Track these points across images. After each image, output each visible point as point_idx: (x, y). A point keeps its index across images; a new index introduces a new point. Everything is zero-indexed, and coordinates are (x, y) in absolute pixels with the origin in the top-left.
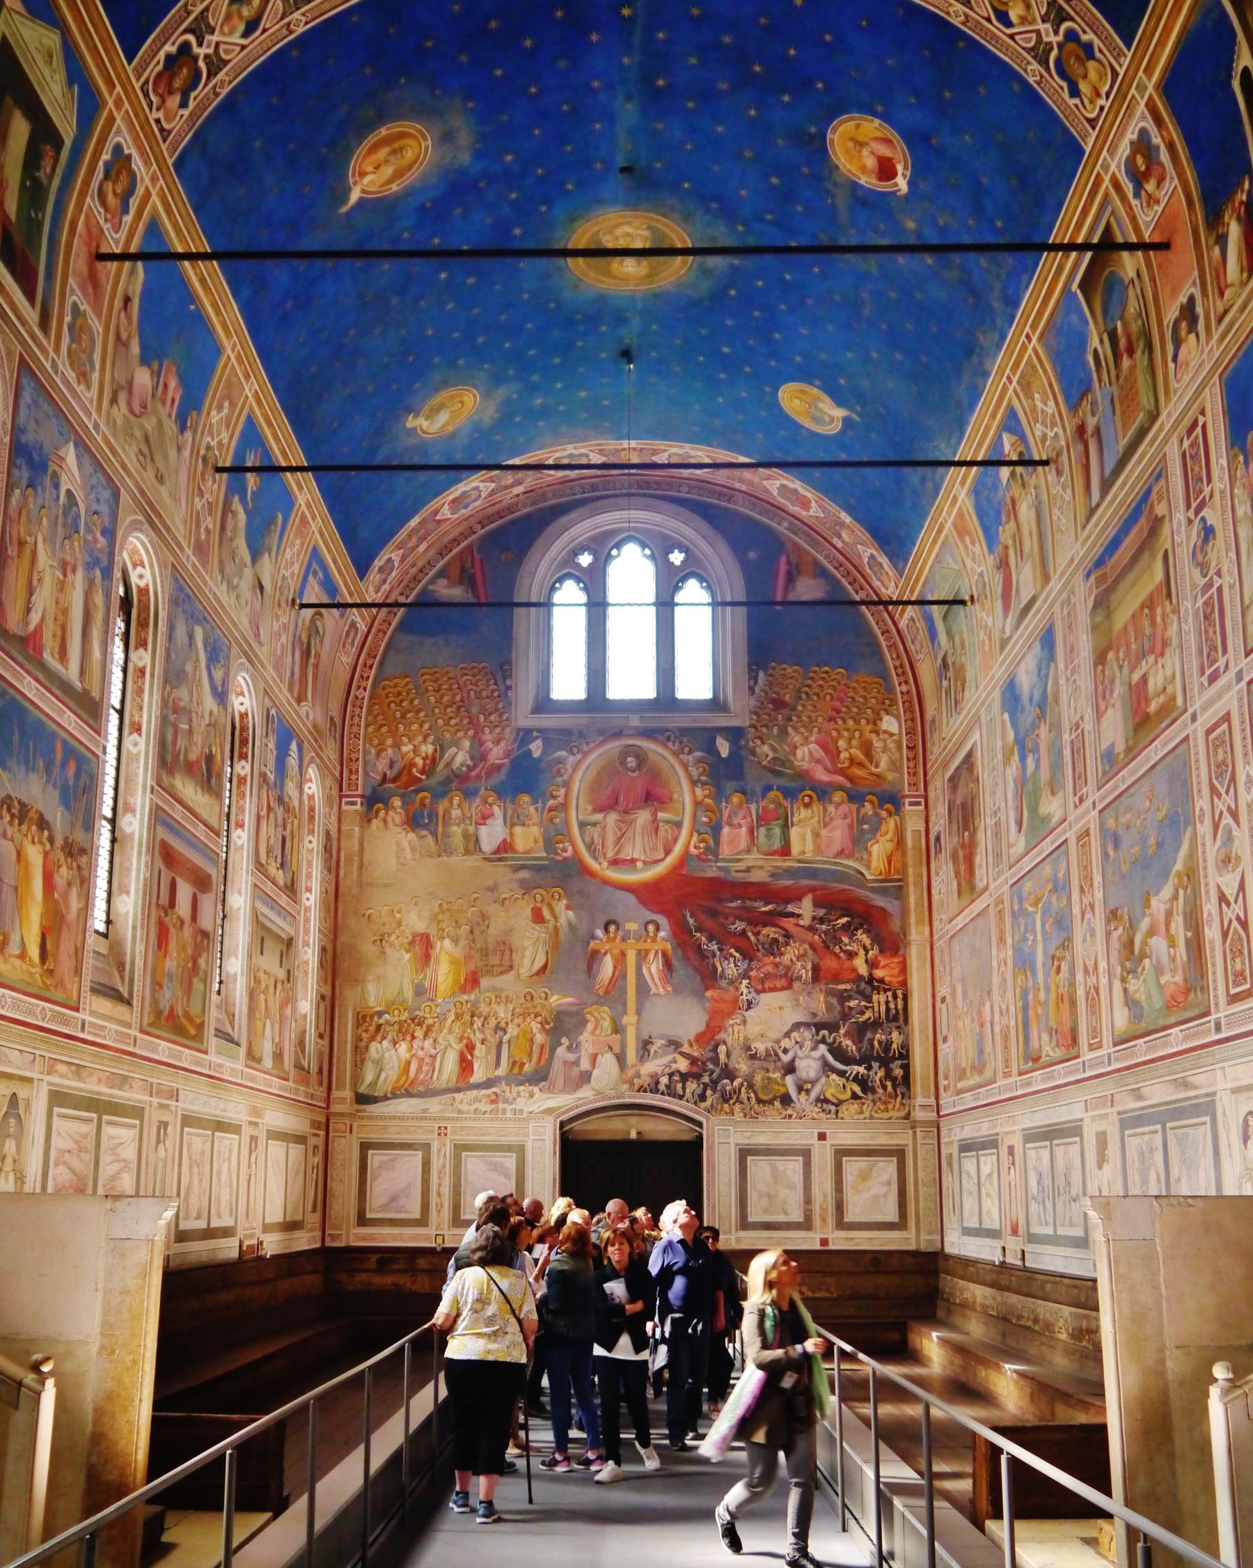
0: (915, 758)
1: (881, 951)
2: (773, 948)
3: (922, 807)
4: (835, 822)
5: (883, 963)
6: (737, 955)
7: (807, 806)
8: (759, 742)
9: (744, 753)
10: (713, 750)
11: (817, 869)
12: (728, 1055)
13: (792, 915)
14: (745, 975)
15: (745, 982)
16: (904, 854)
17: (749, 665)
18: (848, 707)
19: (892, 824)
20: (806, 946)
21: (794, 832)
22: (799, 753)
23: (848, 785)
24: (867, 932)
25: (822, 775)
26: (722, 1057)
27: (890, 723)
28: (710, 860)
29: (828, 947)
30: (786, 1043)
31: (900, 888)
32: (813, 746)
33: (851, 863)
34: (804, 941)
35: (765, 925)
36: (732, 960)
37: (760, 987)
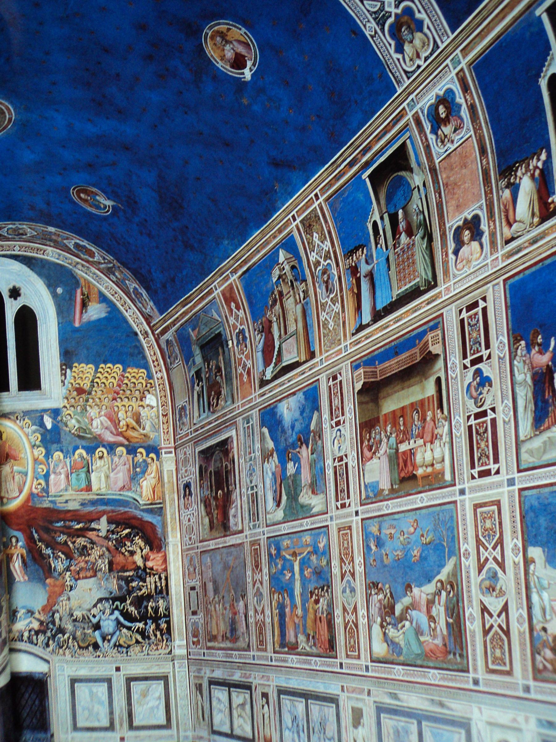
0: (167, 422)
1: (151, 549)
2: (84, 551)
3: (173, 454)
4: (119, 468)
5: (151, 558)
6: (63, 556)
7: (101, 458)
8: (69, 418)
9: (60, 425)
10: (42, 424)
11: (108, 499)
12: (61, 619)
13: (94, 530)
14: (68, 569)
15: (68, 573)
16: (163, 486)
17: (61, 366)
18: (124, 390)
19: (155, 467)
20: (104, 549)
21: (93, 476)
22: (95, 423)
23: (126, 443)
24: (141, 538)
25: (110, 438)
26: (57, 620)
27: (151, 400)
28: (44, 496)
29: (117, 549)
30: (94, 611)
31: (162, 508)
32: (103, 419)
33: (130, 494)
34: (102, 546)
35: (78, 537)
36: (60, 560)
37: (77, 577)
